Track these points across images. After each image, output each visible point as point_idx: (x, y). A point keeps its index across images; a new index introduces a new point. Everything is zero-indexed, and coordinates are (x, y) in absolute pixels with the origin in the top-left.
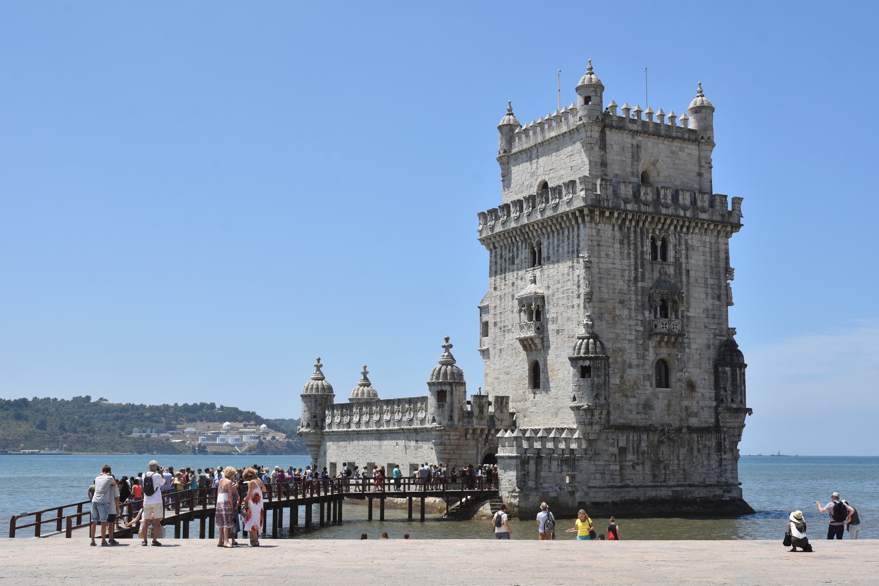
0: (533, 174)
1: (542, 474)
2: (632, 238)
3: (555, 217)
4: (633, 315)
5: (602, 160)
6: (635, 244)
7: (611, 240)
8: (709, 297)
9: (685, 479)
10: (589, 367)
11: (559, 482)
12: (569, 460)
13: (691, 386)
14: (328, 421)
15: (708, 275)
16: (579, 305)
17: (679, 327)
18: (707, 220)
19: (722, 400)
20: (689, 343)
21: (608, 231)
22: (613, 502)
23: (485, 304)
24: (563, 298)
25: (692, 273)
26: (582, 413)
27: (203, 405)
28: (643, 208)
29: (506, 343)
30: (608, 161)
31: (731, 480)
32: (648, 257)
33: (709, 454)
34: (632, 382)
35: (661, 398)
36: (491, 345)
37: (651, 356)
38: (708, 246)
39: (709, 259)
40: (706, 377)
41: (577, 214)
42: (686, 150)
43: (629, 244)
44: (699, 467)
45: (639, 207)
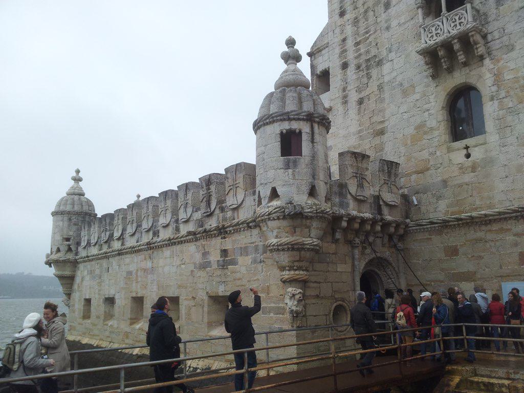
14: (83, 244)
36: (340, 101)
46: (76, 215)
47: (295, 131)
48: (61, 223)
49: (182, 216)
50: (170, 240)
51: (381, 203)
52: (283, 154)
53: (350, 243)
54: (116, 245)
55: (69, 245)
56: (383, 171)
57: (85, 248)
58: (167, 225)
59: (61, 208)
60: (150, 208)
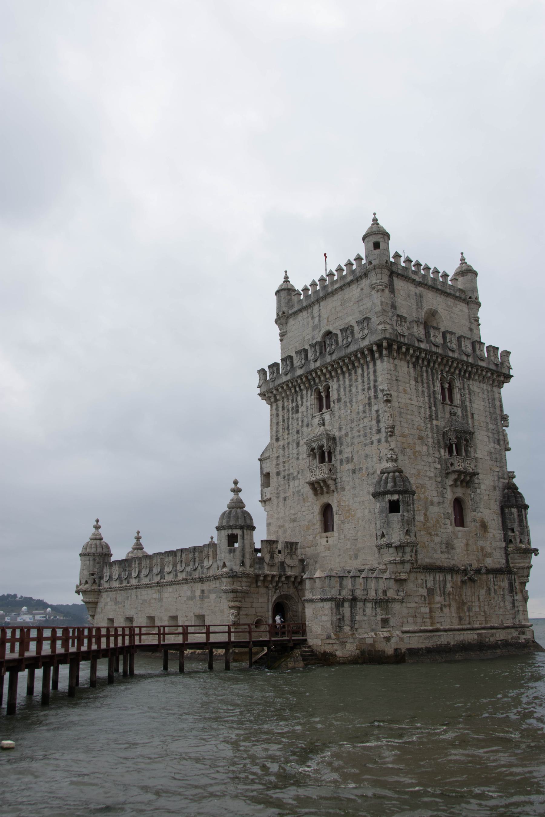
0: (314, 328)
1: (357, 618)
2: (425, 377)
3: (348, 356)
4: (431, 452)
5: (392, 302)
6: (427, 383)
7: (407, 376)
8: (491, 440)
10: (398, 501)
11: (374, 627)
12: (382, 603)
13: (484, 526)
14: (106, 579)
16: (379, 441)
17: (472, 466)
18: (486, 368)
19: (511, 541)
20: (479, 483)
21: (405, 369)
22: (426, 648)
23: (267, 455)
24: (359, 436)
25: (475, 416)
26: (392, 550)
27: (9, 595)
28: (434, 349)
29: (291, 490)
30: (398, 305)
31: (524, 623)
32: (440, 397)
34: (435, 520)
35: (460, 537)
36: (275, 495)
38: (486, 393)
39: (487, 405)
40: (495, 518)
41: (375, 348)
42: (458, 306)
43: (423, 383)
44: (497, 608)
46: (97, 555)
47: (234, 534)
48: (88, 562)
49: (179, 568)
50: (172, 581)
51: (285, 565)
52: (229, 546)
53: (267, 587)
54: (134, 582)
55: (94, 579)
56: (287, 547)
57: (107, 581)
58: (170, 572)
59: (88, 550)
60: (159, 560)
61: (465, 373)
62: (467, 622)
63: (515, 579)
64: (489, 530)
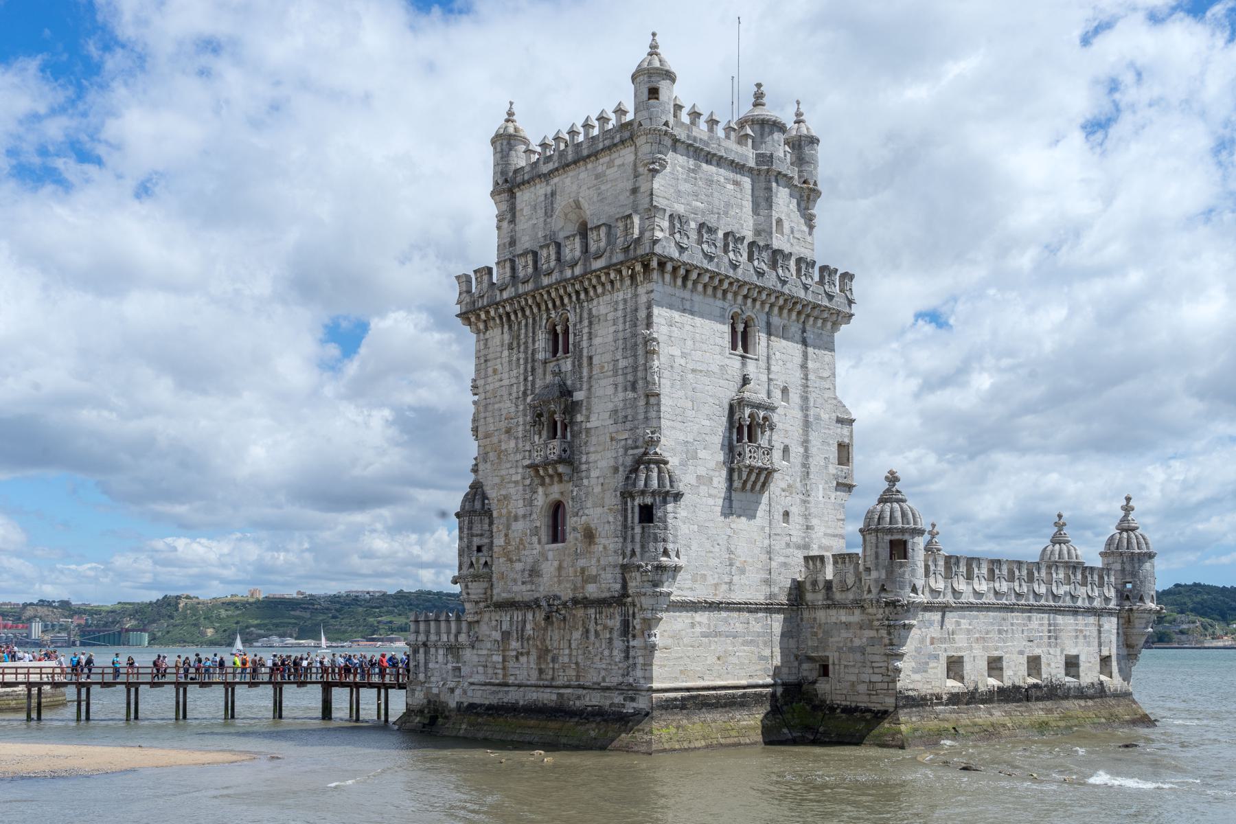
2: (522, 336)
5: (511, 237)
7: (499, 349)
8: (620, 389)
9: (578, 677)
13: (590, 535)
15: (619, 355)
17: (557, 451)
20: (588, 470)
30: (518, 235)
33: (611, 639)
37: (540, 500)
38: (621, 306)
39: (621, 327)
40: (611, 519)
43: (519, 346)
45: (516, 290)
61: (578, 293)
62: (549, 677)
63: (634, 613)
64: (597, 540)
